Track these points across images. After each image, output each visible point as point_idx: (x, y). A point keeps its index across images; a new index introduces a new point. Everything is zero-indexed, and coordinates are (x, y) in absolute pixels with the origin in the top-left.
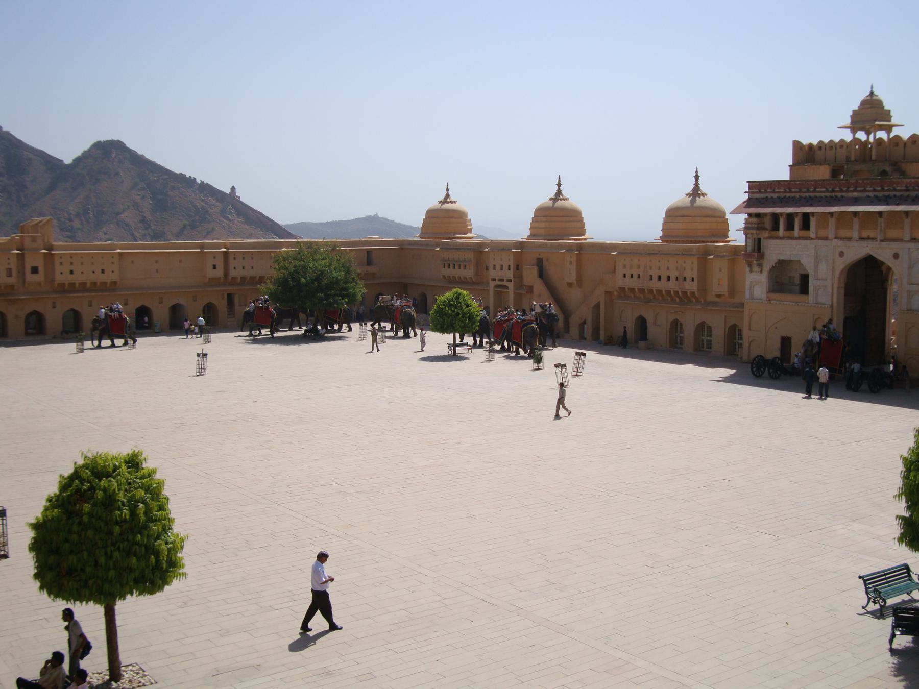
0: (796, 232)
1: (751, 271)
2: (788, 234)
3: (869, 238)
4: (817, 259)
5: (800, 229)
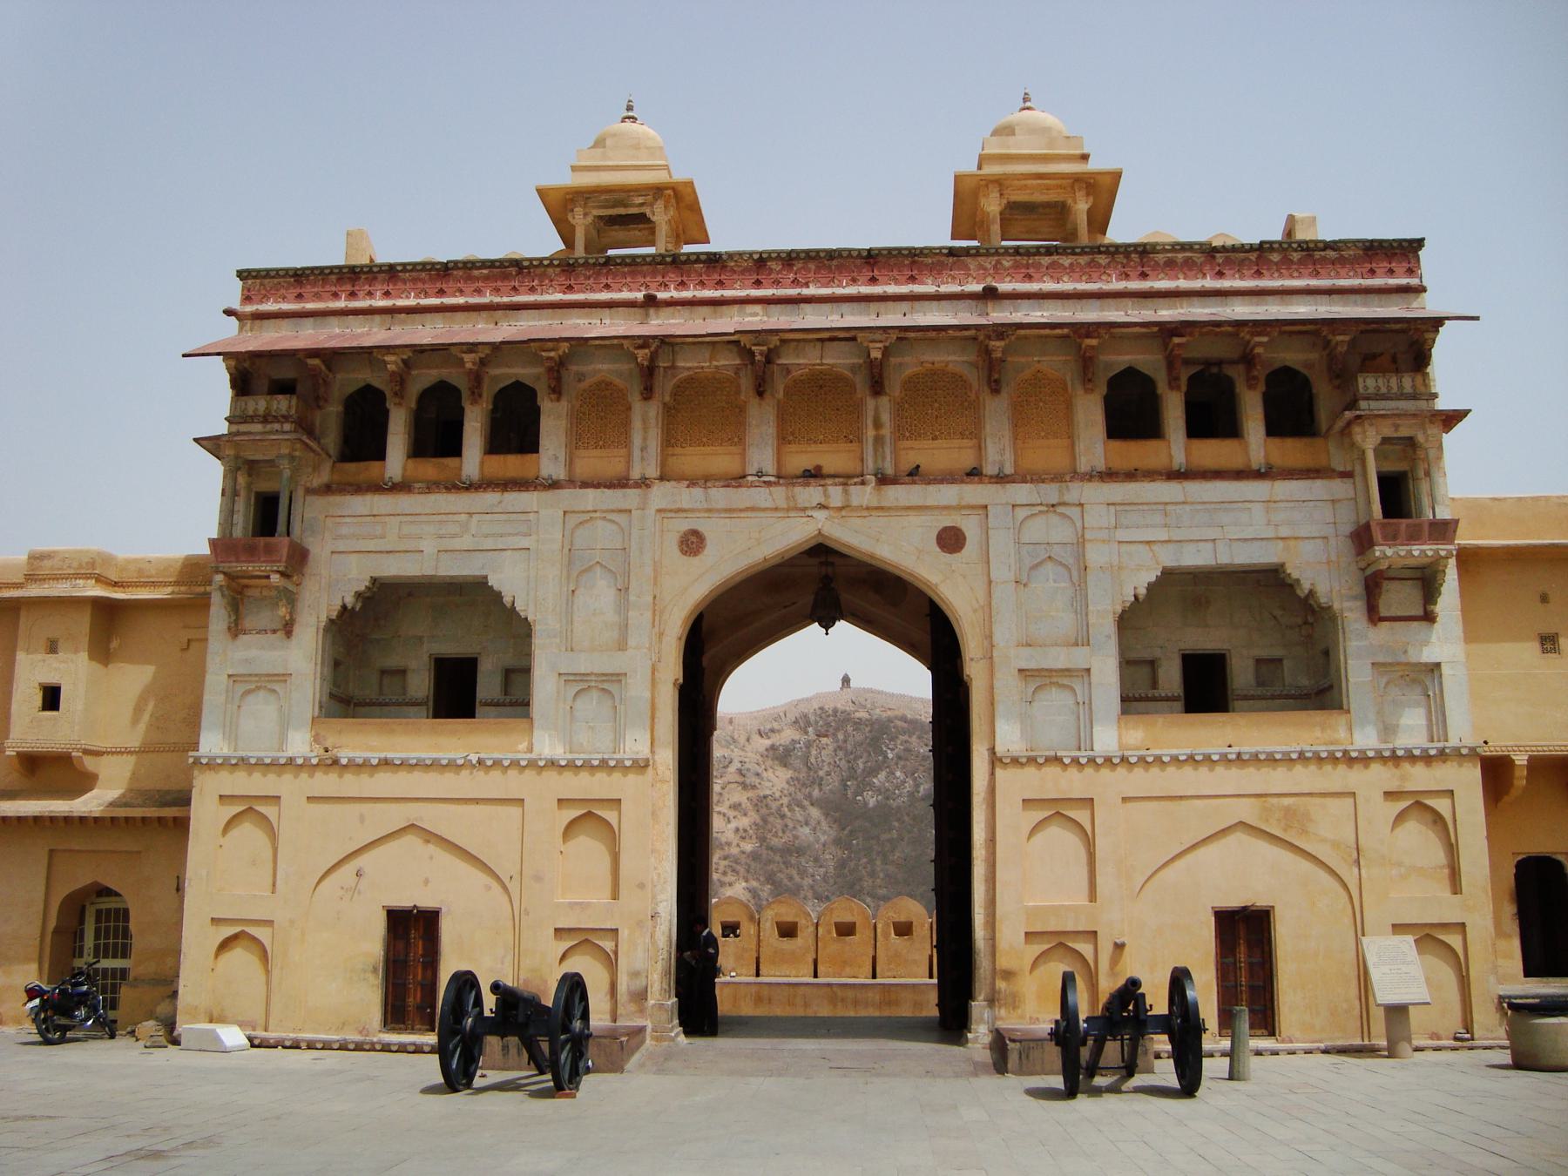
0: (473, 457)
1: (236, 630)
2: (429, 468)
3: (813, 475)
4: (576, 568)
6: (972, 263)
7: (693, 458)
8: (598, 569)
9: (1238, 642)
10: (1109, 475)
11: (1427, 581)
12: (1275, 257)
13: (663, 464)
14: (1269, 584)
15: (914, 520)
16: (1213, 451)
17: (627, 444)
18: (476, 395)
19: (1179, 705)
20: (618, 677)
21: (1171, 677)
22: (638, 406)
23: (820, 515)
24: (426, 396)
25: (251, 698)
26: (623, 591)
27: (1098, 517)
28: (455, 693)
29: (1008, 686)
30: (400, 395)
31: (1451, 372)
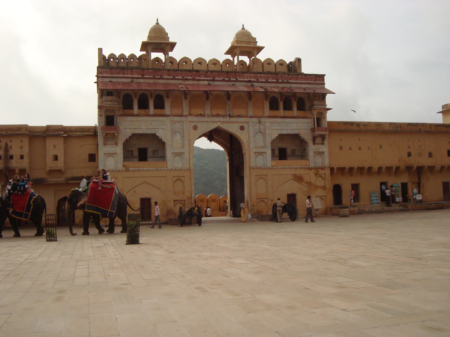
0: (152, 110)
1: (105, 144)
2: (142, 112)
3: (218, 115)
4: (174, 133)
5: (156, 107)
6: (246, 75)
7: (195, 111)
8: (177, 133)
9: (289, 146)
10: (270, 117)
11: (323, 137)
12: (300, 76)
13: (189, 112)
14: (296, 137)
15: (235, 124)
16: (288, 113)
17: (182, 107)
18: (152, 96)
19: (278, 158)
20: (183, 153)
21: (277, 152)
22: (184, 100)
23: (219, 123)
24: (141, 96)
25: (108, 158)
26: (183, 137)
27: (268, 125)
28: (143, 156)
29: (252, 154)
30: (136, 97)
31: (329, 100)
